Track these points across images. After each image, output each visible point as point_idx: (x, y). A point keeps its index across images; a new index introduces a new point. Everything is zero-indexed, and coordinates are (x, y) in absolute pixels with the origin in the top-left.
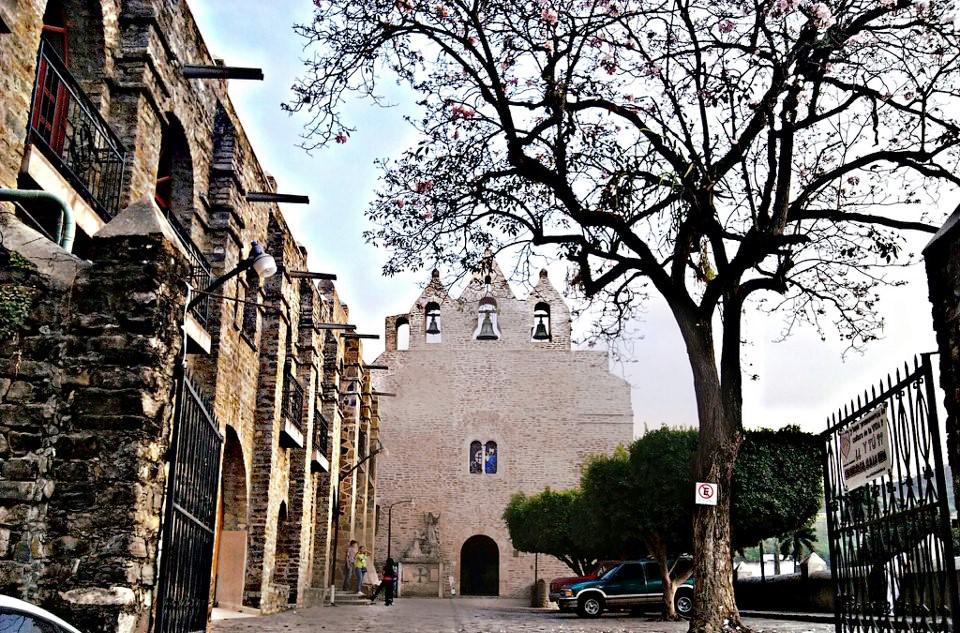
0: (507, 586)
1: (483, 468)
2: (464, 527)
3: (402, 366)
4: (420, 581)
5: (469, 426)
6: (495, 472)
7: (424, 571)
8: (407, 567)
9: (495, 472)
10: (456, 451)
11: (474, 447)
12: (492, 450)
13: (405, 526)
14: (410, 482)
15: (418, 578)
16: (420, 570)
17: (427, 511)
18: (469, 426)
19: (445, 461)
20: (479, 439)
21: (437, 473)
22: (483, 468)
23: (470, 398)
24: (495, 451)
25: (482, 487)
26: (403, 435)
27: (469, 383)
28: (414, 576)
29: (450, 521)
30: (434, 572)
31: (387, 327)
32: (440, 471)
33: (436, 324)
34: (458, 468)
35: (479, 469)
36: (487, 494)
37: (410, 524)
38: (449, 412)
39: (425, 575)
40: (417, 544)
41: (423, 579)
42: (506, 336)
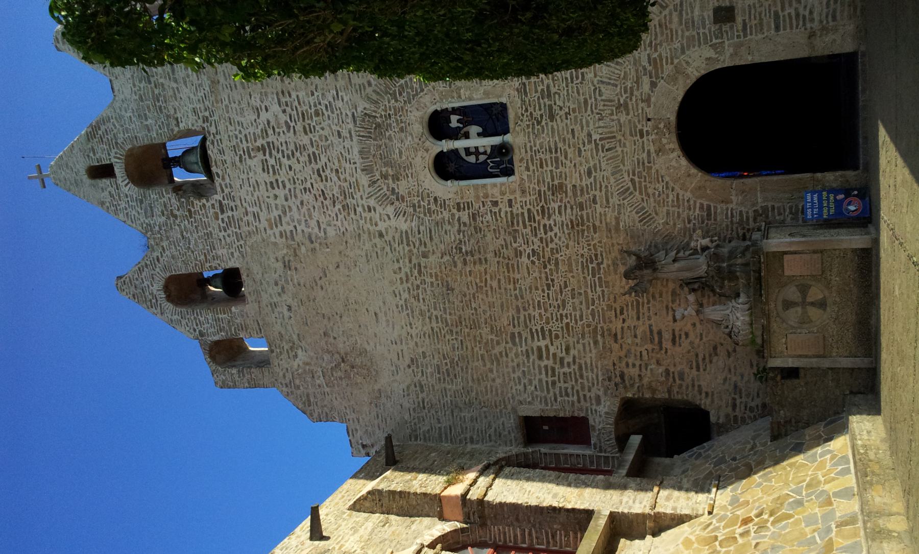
0: (825, 30)
1: (496, 140)
2: (659, 178)
3: (300, 352)
4: (822, 304)
5: (403, 187)
6: (503, 107)
7: (792, 293)
8: (779, 343)
9: (503, 107)
10: (465, 217)
11: (452, 167)
12: (454, 121)
13: (667, 336)
14: (555, 326)
15: (813, 312)
16: (788, 305)
17: (621, 284)
18: (403, 187)
19: (492, 242)
20: (430, 158)
21: (524, 260)
22: (496, 140)
23: (336, 191)
24: (455, 111)
25: (546, 139)
26: (447, 349)
27: (306, 197)
28: (805, 321)
29: (646, 218)
30: (793, 267)
31: (235, 386)
32: (518, 254)
33: (215, 276)
34: (504, 207)
35: (503, 151)
36: (560, 124)
37: (662, 322)
38: (377, 240)
39: (804, 290)
40: (714, 312)
41: (816, 293)
42: (192, 118)
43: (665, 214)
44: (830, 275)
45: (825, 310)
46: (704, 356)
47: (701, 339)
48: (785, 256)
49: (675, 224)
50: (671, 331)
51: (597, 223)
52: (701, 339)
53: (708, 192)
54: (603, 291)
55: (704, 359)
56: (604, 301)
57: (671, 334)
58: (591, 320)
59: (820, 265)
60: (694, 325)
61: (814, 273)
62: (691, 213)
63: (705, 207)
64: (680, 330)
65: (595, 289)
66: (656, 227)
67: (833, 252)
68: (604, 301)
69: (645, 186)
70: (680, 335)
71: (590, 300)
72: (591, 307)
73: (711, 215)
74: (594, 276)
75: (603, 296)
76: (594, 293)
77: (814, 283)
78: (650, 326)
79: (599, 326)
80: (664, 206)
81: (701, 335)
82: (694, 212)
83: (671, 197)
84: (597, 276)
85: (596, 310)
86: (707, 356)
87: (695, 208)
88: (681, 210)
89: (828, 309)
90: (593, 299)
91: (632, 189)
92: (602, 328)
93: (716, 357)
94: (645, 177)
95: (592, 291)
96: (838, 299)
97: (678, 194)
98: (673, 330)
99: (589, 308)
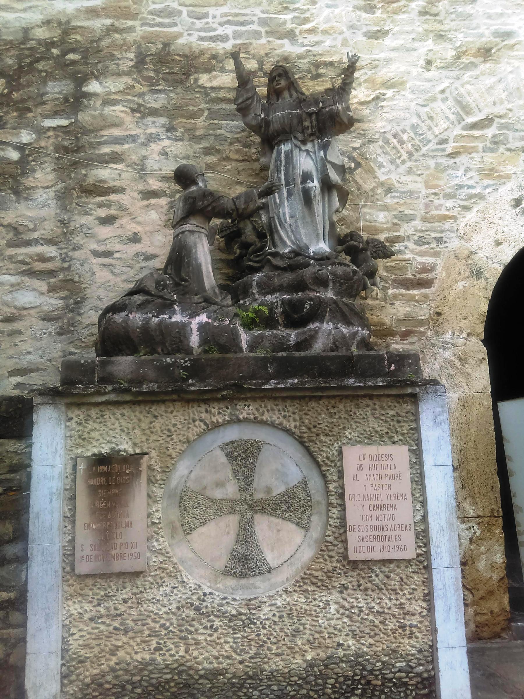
43: (410, 187)
44: (345, 587)
45: (227, 572)
46: (50, 259)
47: (96, 254)
48: (405, 449)
49: (385, 208)
50: (118, 184)
51: (388, 41)
52: (96, 254)
53: (461, 284)
54: (224, 39)
55: (42, 259)
56: (201, 39)
57: (112, 184)
58: (152, 7)
59: (378, 556)
60: (135, 239)
61: (352, 539)
62: (411, 245)
63: (425, 276)
64: (122, 208)
65: (228, 22)
66: (381, 166)
67: (419, 594)
68: (201, 39)
69: (474, 150)
70: (109, 206)
71: (206, 9)
72: (184, 10)
73: (408, 288)
74: (263, 22)
75: (211, 39)
76: (219, 19)
77: (315, 533)
78: (133, 138)
79: (136, 23)
80: (427, 187)
81: (108, 254)
82: (412, 251)
83: (449, 203)
84: (263, 30)
85: (176, 19)
86: (49, 266)
87: (422, 254)
88: (418, 223)
89: (231, 582)
90: (205, 16)
91: (471, 120)
92: (131, 29)
93: (44, 287)
94: (492, 150)
95: (225, 15)
96: (265, 612)
97: (454, 218)
98: (120, 190)
99: (181, 5)
